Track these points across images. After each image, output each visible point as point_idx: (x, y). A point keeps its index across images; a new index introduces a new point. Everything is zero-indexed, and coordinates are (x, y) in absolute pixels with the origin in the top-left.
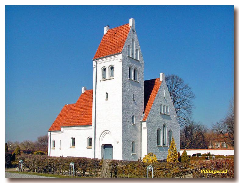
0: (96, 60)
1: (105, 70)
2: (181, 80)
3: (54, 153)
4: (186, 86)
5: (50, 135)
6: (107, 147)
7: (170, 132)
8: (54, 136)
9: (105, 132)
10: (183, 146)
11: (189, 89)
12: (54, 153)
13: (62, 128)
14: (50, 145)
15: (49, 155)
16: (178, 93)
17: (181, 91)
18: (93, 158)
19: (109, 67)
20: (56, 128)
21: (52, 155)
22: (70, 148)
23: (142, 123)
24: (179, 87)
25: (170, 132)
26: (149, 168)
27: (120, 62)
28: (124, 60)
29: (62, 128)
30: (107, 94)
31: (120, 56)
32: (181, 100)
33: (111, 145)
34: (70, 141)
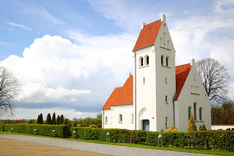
0: (135, 51)
1: (142, 59)
2: (217, 62)
3: (106, 126)
4: (222, 68)
5: (103, 112)
6: (145, 122)
7: (200, 109)
8: (107, 113)
9: (143, 110)
10: (215, 122)
11: (225, 71)
12: (106, 126)
13: (112, 108)
14: (103, 121)
15: (102, 128)
16: (214, 75)
17: (217, 72)
18: (135, 129)
19: (145, 57)
20: (107, 106)
21: (46, 120)
22: (119, 123)
23: (174, 101)
24: (216, 69)
25: (200, 109)
26: (159, 137)
27: (153, 52)
28: (156, 50)
29: (112, 108)
30: (144, 78)
31: (153, 48)
32: (217, 80)
33: (148, 120)
34: (118, 118)
